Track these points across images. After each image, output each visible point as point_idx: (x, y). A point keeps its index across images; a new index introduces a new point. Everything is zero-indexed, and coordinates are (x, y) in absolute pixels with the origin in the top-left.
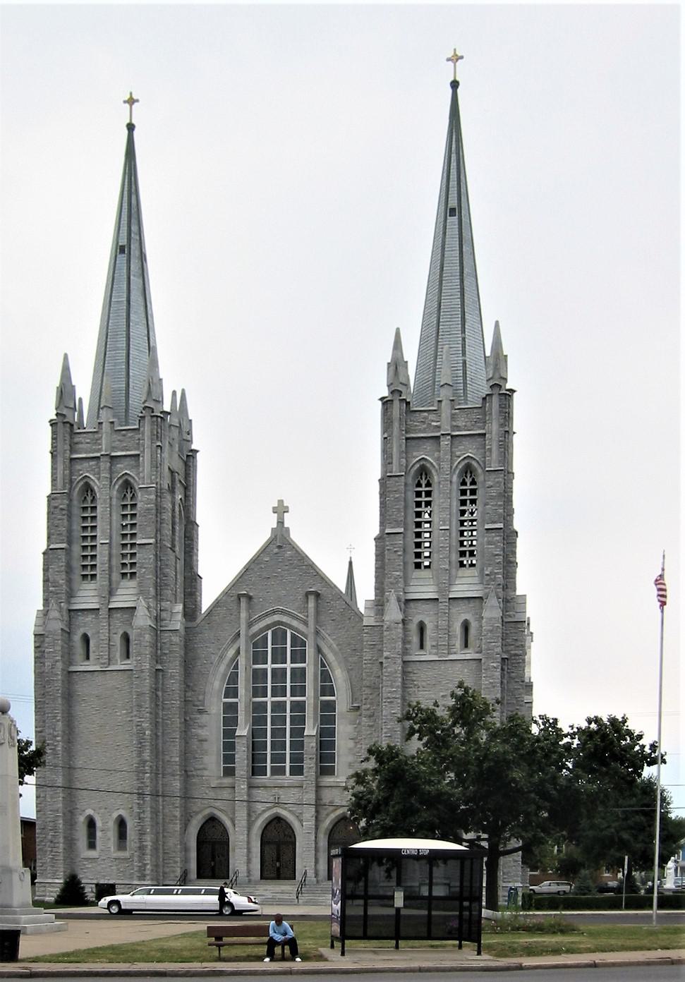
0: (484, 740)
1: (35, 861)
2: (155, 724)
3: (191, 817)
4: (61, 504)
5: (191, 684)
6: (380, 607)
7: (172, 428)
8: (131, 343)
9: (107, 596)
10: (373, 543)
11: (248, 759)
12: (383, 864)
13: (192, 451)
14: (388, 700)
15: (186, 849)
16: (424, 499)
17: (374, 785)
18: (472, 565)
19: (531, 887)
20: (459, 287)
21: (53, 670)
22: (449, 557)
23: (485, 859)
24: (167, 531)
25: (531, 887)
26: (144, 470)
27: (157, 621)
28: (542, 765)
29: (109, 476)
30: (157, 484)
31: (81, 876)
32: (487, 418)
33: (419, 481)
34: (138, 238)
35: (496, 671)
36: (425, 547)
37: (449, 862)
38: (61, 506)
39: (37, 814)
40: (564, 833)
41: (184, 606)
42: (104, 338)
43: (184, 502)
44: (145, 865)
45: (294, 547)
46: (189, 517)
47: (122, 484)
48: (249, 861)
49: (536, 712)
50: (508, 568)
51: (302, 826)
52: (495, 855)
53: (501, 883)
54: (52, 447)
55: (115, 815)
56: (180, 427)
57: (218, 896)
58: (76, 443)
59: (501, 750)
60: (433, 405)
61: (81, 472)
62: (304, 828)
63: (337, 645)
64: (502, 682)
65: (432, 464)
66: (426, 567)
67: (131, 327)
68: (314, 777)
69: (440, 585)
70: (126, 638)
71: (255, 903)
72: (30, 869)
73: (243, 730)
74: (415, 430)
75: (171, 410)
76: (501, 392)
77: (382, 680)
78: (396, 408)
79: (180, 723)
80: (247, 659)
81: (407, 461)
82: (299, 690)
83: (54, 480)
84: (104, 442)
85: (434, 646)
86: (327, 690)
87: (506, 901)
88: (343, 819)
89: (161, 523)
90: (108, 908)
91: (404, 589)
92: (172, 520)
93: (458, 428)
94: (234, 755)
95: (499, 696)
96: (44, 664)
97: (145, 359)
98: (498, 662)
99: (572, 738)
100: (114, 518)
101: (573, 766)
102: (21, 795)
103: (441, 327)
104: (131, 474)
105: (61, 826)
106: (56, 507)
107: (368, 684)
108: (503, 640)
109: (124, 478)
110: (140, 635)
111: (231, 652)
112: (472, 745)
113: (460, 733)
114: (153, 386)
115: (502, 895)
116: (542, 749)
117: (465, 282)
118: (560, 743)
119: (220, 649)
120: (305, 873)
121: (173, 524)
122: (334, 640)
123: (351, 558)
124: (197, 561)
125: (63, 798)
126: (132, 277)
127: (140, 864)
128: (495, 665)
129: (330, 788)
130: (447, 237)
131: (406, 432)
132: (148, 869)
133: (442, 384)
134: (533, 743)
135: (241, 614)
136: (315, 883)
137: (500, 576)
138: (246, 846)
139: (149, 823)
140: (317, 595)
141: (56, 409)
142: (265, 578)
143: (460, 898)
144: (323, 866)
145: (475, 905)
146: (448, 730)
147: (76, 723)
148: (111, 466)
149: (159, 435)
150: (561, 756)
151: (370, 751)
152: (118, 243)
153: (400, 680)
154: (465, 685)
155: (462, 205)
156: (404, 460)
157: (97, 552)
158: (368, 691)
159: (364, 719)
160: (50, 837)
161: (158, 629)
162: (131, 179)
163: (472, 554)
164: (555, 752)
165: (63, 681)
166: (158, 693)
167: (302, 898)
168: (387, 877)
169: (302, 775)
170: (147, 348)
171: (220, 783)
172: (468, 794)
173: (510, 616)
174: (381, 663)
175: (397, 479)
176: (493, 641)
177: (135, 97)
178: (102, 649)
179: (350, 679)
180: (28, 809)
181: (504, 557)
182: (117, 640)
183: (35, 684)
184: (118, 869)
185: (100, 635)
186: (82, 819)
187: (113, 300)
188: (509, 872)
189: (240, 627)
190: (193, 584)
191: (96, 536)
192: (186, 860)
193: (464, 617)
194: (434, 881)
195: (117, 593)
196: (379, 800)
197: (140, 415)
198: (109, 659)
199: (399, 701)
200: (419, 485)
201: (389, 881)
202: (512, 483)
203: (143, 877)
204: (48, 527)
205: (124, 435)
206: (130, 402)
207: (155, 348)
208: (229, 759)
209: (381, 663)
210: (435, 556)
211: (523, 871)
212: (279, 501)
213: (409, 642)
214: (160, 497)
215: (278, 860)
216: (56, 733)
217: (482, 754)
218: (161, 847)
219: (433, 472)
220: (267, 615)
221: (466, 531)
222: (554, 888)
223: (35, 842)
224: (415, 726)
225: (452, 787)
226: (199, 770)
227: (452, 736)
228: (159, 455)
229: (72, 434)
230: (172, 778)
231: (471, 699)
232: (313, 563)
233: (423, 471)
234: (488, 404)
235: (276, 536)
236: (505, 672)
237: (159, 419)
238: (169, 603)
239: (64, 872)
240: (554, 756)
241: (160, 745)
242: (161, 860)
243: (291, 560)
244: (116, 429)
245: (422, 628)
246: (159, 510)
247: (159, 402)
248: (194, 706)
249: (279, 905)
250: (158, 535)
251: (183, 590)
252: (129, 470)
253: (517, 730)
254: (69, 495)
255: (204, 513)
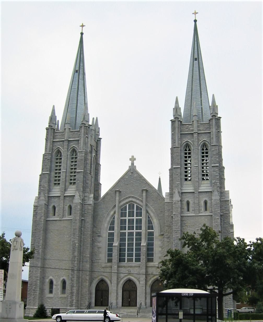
0: (215, 247)
1: (26, 299)
2: (80, 241)
3: (93, 279)
4: (48, 157)
5: (96, 225)
6: (171, 195)
7: (92, 130)
8: (78, 102)
9: (64, 191)
10: (169, 171)
11: (118, 255)
12: (174, 300)
13: (99, 138)
14: (175, 231)
15: (91, 294)
16: (188, 155)
17: (170, 266)
18: (207, 179)
19: (237, 310)
20: (199, 83)
21: (40, 220)
22: (198, 176)
23: (217, 297)
24: (88, 167)
25: (237, 310)
26: (81, 145)
27: (83, 201)
28: (239, 258)
29: (67, 147)
30: (85, 150)
31: (45, 305)
32: (211, 127)
33: (186, 149)
34: (83, 68)
35: (218, 220)
36: (189, 173)
37: (202, 299)
38: (48, 158)
39: (29, 278)
40: (250, 286)
41: (94, 195)
42: (68, 100)
43: (95, 157)
44: (73, 300)
45: (137, 173)
46: (97, 162)
47: (72, 150)
48: (117, 298)
49: (235, 236)
50: (221, 180)
51: (140, 283)
52: (221, 295)
53: (224, 308)
54: (46, 137)
55: (62, 279)
56: (95, 130)
57: (103, 314)
58: (56, 136)
59: (222, 251)
60: (190, 123)
61: (57, 146)
62: (141, 284)
63: (155, 210)
64: (221, 224)
65: (191, 143)
66: (189, 180)
67: (78, 97)
68: (145, 263)
69: (195, 187)
70: (70, 207)
71: (119, 317)
72: (24, 302)
73: (116, 244)
74: (184, 131)
75: (92, 124)
76: (216, 118)
77: (173, 223)
78: (177, 124)
79: (90, 241)
80: (118, 215)
81: (181, 142)
82: (139, 228)
83: (46, 149)
84: (66, 135)
85: (193, 210)
86: (150, 227)
87: (227, 316)
88: (157, 280)
89: (86, 164)
90: (56, 319)
91: (181, 188)
92: (91, 163)
93: (200, 130)
94: (112, 253)
95: (220, 229)
96: (37, 217)
97: (83, 107)
98: (219, 216)
99: (251, 247)
100: (68, 162)
101: (252, 258)
102: (23, 271)
103: (193, 96)
104: (76, 146)
105: (38, 283)
106: (46, 159)
107: (167, 225)
108: (220, 208)
109: (73, 148)
110: (76, 206)
111: (112, 213)
112: (210, 249)
113: (205, 245)
114: (86, 116)
115: (225, 313)
116: (239, 251)
117: (201, 82)
118: (246, 248)
119: (107, 211)
120: (141, 304)
121: (91, 164)
122: (153, 208)
123: (160, 177)
124: (100, 178)
125: (40, 271)
126: (80, 80)
127: (71, 300)
128: (218, 217)
129: (151, 267)
130: (194, 67)
131: (181, 132)
132: (74, 302)
133: (194, 115)
134: (235, 249)
135: (116, 198)
136: (145, 308)
137: (218, 183)
138: (116, 292)
139: (75, 282)
140: (147, 191)
141: (49, 124)
142: (127, 184)
143: (208, 315)
144: (148, 301)
145: (214, 318)
146: (200, 243)
147: (48, 241)
148: (68, 144)
149: (87, 133)
150: (247, 254)
151: (168, 252)
152: (75, 69)
153: (180, 223)
154: (206, 225)
155: (199, 57)
156: (180, 142)
157: (61, 175)
158: (167, 228)
159: (165, 239)
160: (33, 288)
161: (83, 204)
162: (81, 50)
163: (207, 175)
164: (244, 252)
165: (44, 224)
166: (82, 228)
167: (140, 315)
168: (176, 306)
169: (140, 262)
170: (84, 103)
171: (106, 265)
172: (209, 270)
173: (223, 199)
174: (172, 217)
175: (177, 148)
176: (217, 208)
177: (84, 25)
178: (61, 211)
179: (160, 223)
180: (25, 276)
181: (219, 176)
182: (67, 208)
183: (33, 225)
184: (61, 302)
185: (60, 206)
186: (47, 281)
187: (72, 87)
188: (227, 303)
189: (116, 203)
190: (98, 187)
191: (61, 169)
192: (90, 298)
193: (204, 199)
194: (196, 307)
195: (68, 190)
196: (172, 272)
197: (80, 126)
198: (63, 215)
199: (180, 232)
200: (186, 150)
201: (176, 307)
202: (221, 149)
203: (71, 306)
204: (42, 166)
205: (74, 133)
206: (77, 122)
207: (87, 104)
208: (110, 255)
209: (172, 217)
210: (193, 176)
211: (234, 302)
212: (132, 156)
213: (183, 209)
214: (87, 155)
215: (129, 298)
216: (39, 245)
217: (214, 253)
218: (80, 292)
219: (191, 146)
220: (127, 198)
221: (204, 167)
222: (247, 310)
223: (27, 290)
224: (186, 242)
225: (202, 267)
226: (97, 260)
227: (202, 246)
228: (87, 140)
229: (54, 132)
230: (86, 263)
231: (209, 231)
232: (145, 179)
233: (187, 145)
234: (211, 122)
235: (131, 169)
236: (222, 220)
237: (87, 127)
238: (88, 194)
239: (38, 303)
240: (244, 254)
241: (82, 250)
242: (80, 298)
243: (136, 178)
244: (71, 131)
245: (188, 203)
246: (86, 159)
247: (88, 121)
248: (96, 234)
249: (129, 318)
250: (85, 169)
251: (94, 189)
252: (75, 145)
253: (228, 243)
254: (51, 154)
255: (103, 161)
